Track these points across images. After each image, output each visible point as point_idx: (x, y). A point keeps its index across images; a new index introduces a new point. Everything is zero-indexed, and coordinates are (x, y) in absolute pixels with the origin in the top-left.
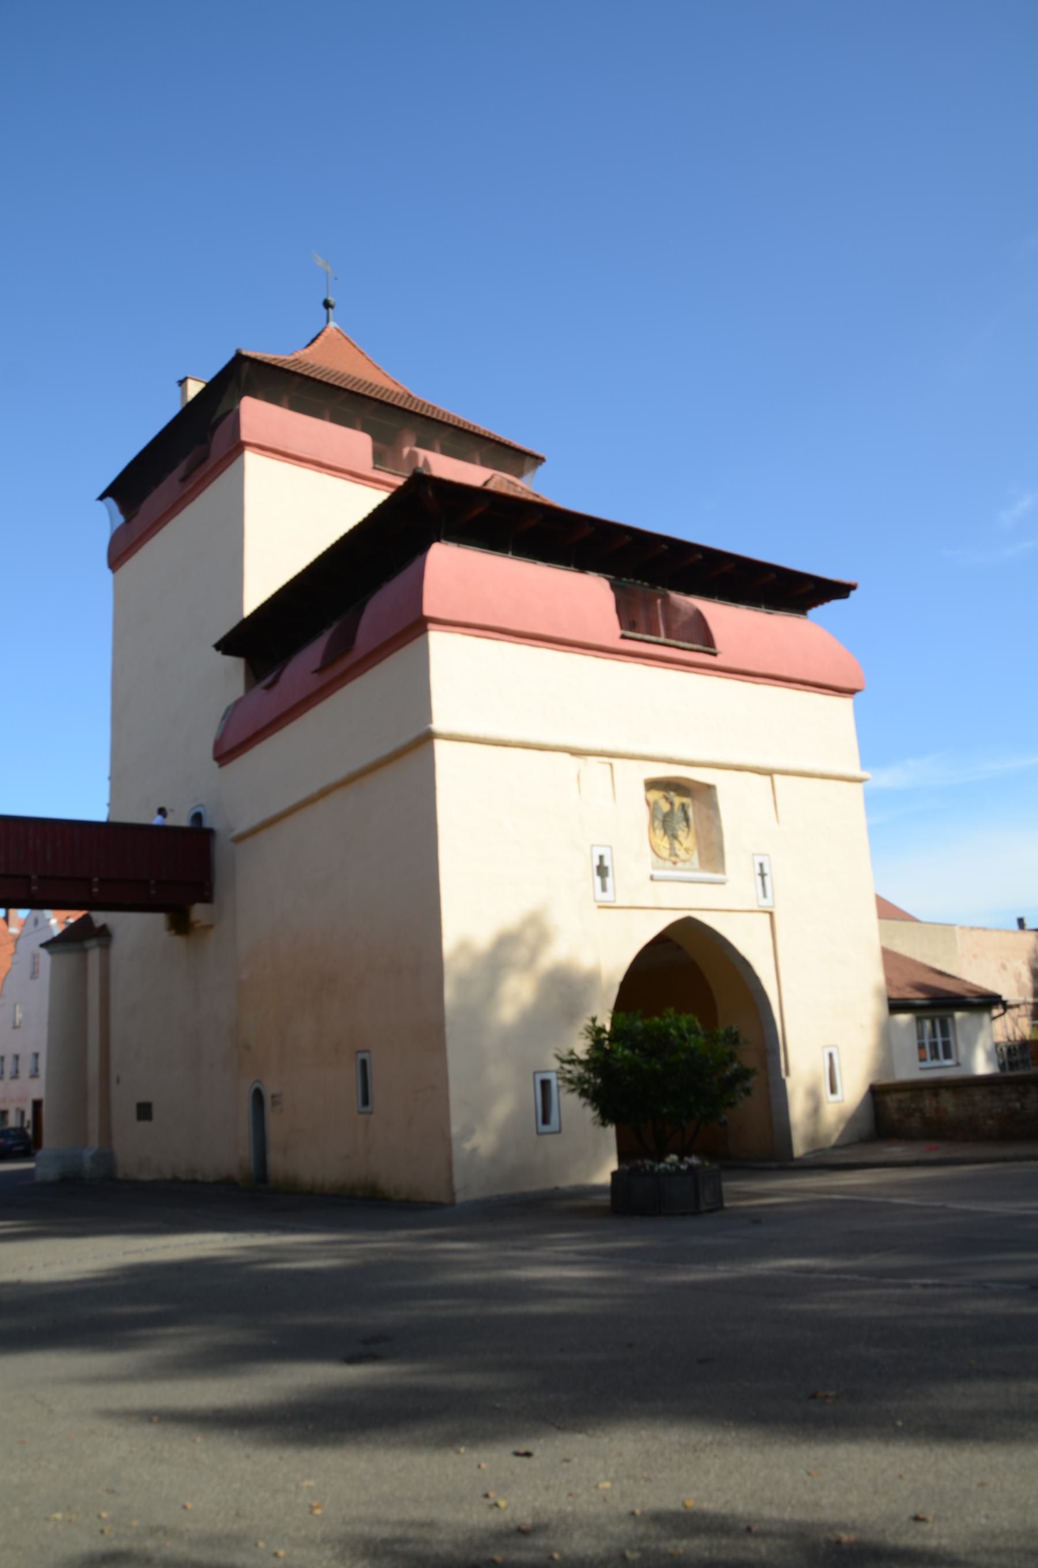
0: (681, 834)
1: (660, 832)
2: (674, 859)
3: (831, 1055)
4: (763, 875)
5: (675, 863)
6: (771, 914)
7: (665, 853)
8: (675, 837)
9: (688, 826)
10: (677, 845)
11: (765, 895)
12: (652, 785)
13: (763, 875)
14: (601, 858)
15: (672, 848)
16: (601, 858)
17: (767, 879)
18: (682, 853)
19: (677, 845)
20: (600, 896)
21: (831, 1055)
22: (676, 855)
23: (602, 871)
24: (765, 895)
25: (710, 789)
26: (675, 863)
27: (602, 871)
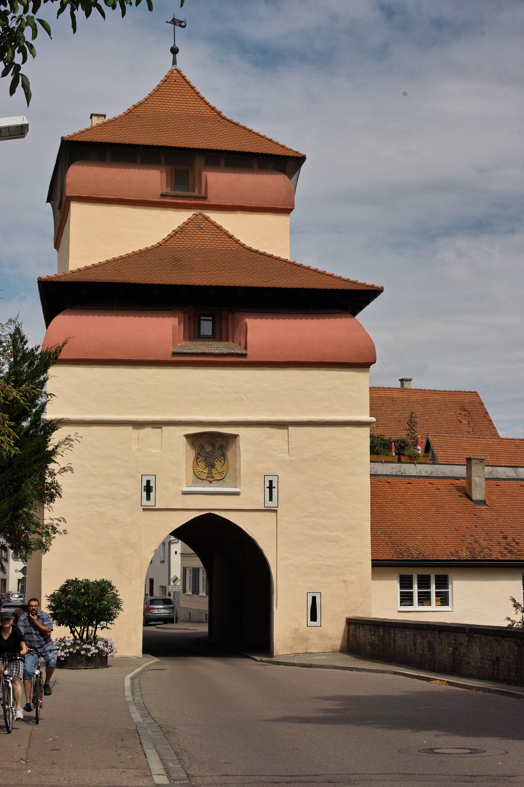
0: (218, 465)
1: (202, 465)
2: (209, 479)
3: (314, 598)
4: (271, 487)
5: (210, 482)
6: (276, 511)
7: (204, 476)
8: (214, 467)
9: (224, 459)
10: (214, 471)
11: (271, 499)
12: (191, 438)
13: (271, 487)
14: (148, 482)
15: (210, 472)
16: (148, 482)
17: (274, 491)
18: (217, 477)
19: (214, 471)
20: (145, 502)
21: (314, 598)
22: (213, 477)
23: (148, 489)
24: (271, 499)
25: (235, 436)
26: (210, 482)
27: (148, 489)
